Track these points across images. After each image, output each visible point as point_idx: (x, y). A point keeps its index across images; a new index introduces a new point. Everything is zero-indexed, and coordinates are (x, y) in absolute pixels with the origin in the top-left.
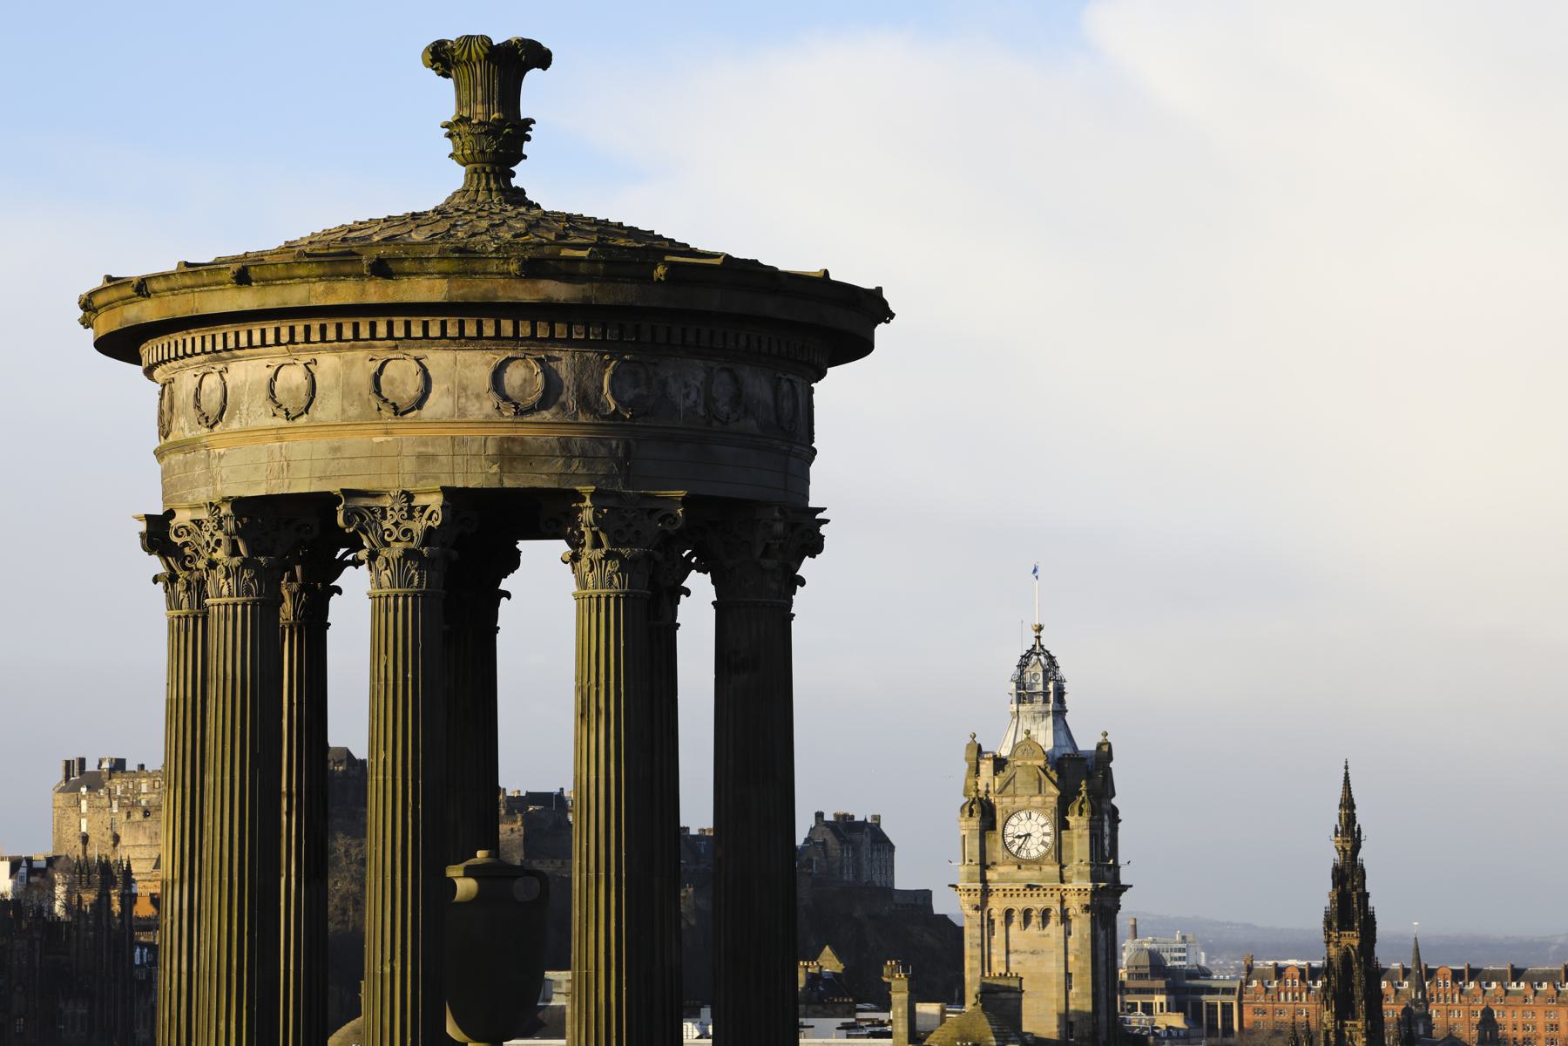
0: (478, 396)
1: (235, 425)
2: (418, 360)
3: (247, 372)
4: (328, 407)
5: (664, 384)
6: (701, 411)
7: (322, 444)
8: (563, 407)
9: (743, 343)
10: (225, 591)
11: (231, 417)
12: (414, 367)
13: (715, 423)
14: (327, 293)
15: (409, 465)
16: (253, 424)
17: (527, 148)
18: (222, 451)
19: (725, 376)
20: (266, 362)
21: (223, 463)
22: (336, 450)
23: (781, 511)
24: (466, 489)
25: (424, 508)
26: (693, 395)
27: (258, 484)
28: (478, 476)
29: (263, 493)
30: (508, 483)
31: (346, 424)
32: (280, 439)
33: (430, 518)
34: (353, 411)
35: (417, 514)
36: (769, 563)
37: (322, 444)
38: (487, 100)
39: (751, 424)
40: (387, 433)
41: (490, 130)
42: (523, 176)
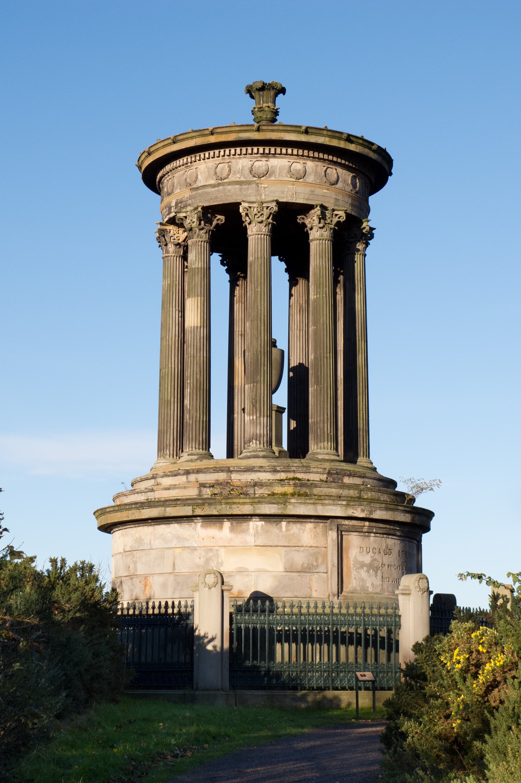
0: (347, 185)
1: (273, 178)
3: (275, 162)
4: (310, 178)
7: (308, 190)
10: (264, 230)
11: (271, 176)
14: (329, 141)
16: (280, 179)
18: (266, 186)
20: (287, 160)
21: (266, 189)
22: (313, 191)
25: (336, 215)
27: (284, 198)
29: (284, 200)
30: (353, 213)
32: (293, 185)
33: (339, 218)
34: (318, 181)
35: (334, 216)
37: (308, 190)
40: (328, 190)
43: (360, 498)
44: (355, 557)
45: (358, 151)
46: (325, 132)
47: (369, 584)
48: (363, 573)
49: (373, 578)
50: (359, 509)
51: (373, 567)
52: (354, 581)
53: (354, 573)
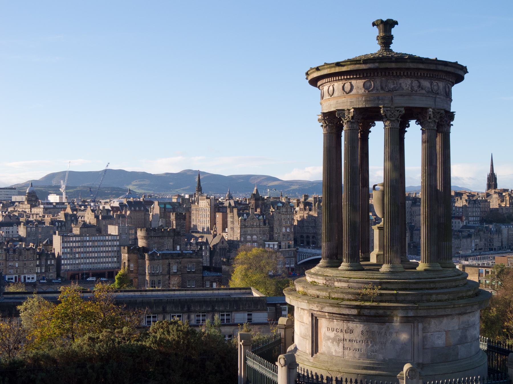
2: (350, 83)
4: (336, 94)
5: (401, 84)
6: (410, 89)
7: (335, 101)
8: (378, 90)
9: (419, 74)
12: (349, 84)
13: (414, 92)
15: (349, 104)
17: (393, 41)
19: (416, 82)
23: (433, 109)
24: (359, 108)
26: (408, 86)
28: (361, 105)
30: (367, 106)
31: (339, 97)
34: (340, 94)
36: (429, 120)
37: (335, 101)
38: (383, 32)
39: (424, 92)
41: (383, 38)
42: (392, 47)
43: (329, 297)
44: (325, 333)
45: (349, 69)
46: (326, 67)
47: (333, 350)
48: (329, 343)
49: (336, 347)
50: (315, 306)
51: (337, 341)
52: (324, 347)
53: (324, 342)
